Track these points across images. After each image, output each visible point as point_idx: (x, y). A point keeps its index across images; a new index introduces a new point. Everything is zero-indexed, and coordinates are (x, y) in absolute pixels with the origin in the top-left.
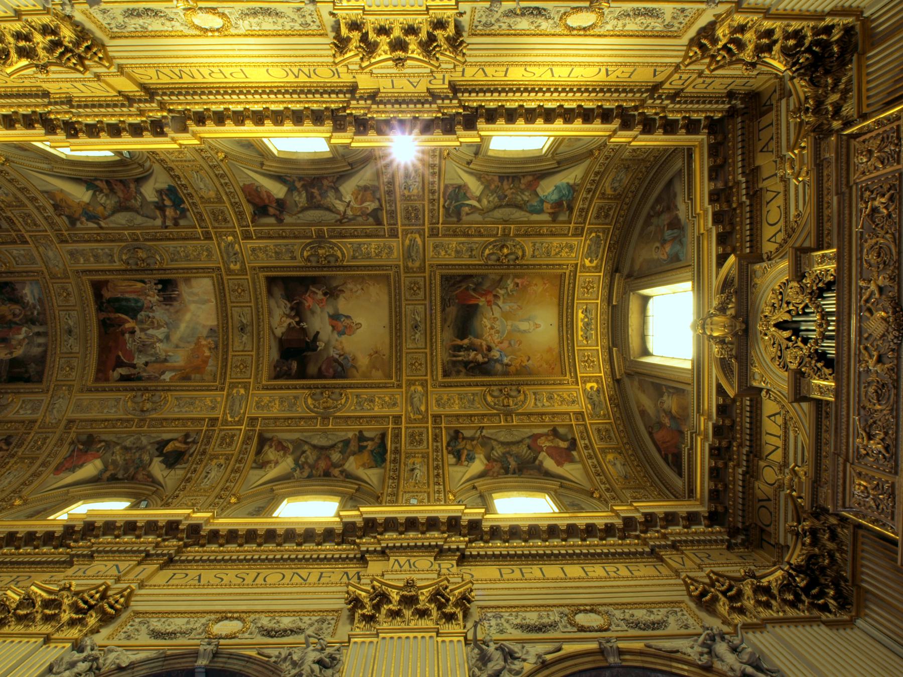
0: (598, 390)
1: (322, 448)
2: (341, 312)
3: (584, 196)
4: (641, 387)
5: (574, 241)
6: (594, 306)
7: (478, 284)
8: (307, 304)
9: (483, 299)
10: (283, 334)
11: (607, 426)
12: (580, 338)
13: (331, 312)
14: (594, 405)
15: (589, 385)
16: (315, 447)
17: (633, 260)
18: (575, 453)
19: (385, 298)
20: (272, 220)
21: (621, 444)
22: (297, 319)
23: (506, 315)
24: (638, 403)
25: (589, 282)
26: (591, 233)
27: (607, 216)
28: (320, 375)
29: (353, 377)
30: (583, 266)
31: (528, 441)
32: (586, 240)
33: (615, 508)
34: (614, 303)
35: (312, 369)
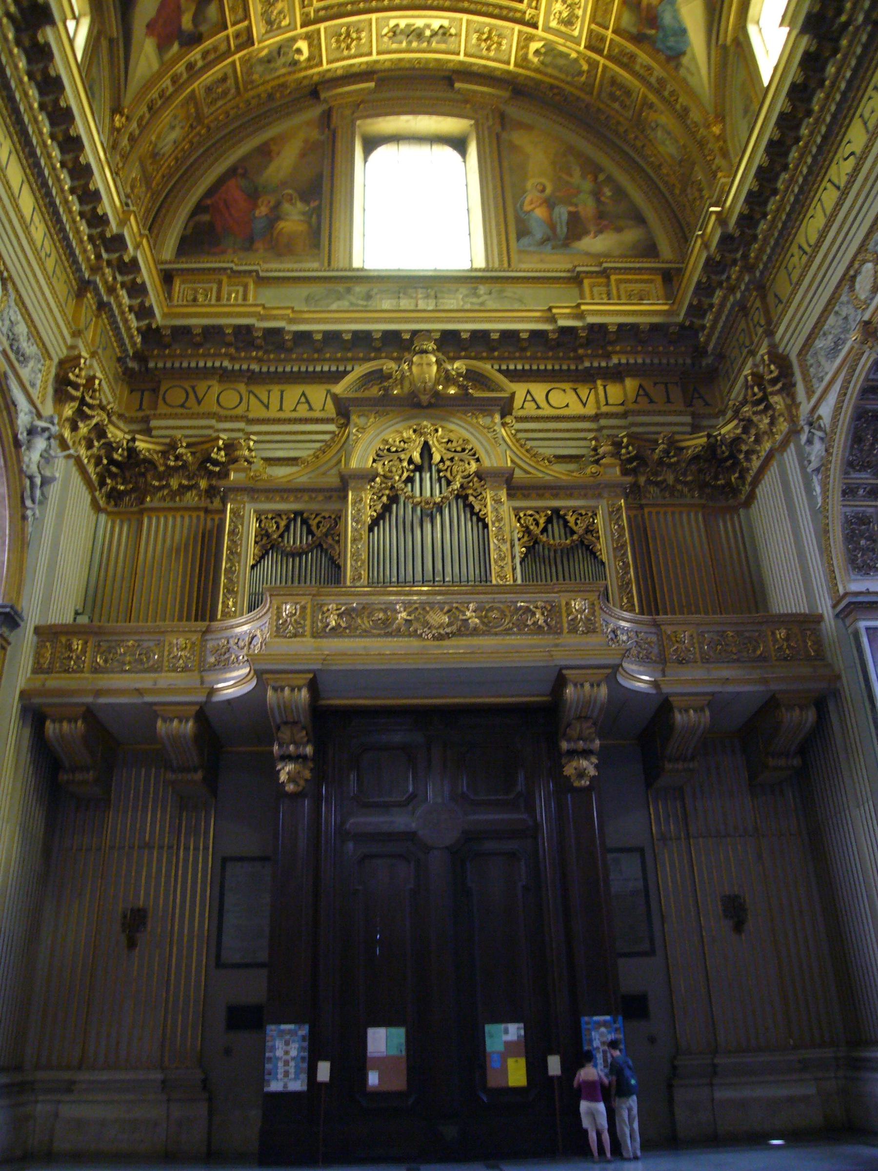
0: (295, 63)
3: (656, 74)
4: (309, 149)
5: (580, 30)
6: (452, 47)
11: (233, 91)
12: (392, 23)
14: (269, 60)
15: (303, 45)
17: (529, 128)
18: (176, 47)
21: (206, 121)
24: (280, 139)
25: (500, 44)
26: (589, 64)
27: (613, 97)
30: (530, 38)
32: (578, 52)
33: (132, 219)
34: (457, 85)
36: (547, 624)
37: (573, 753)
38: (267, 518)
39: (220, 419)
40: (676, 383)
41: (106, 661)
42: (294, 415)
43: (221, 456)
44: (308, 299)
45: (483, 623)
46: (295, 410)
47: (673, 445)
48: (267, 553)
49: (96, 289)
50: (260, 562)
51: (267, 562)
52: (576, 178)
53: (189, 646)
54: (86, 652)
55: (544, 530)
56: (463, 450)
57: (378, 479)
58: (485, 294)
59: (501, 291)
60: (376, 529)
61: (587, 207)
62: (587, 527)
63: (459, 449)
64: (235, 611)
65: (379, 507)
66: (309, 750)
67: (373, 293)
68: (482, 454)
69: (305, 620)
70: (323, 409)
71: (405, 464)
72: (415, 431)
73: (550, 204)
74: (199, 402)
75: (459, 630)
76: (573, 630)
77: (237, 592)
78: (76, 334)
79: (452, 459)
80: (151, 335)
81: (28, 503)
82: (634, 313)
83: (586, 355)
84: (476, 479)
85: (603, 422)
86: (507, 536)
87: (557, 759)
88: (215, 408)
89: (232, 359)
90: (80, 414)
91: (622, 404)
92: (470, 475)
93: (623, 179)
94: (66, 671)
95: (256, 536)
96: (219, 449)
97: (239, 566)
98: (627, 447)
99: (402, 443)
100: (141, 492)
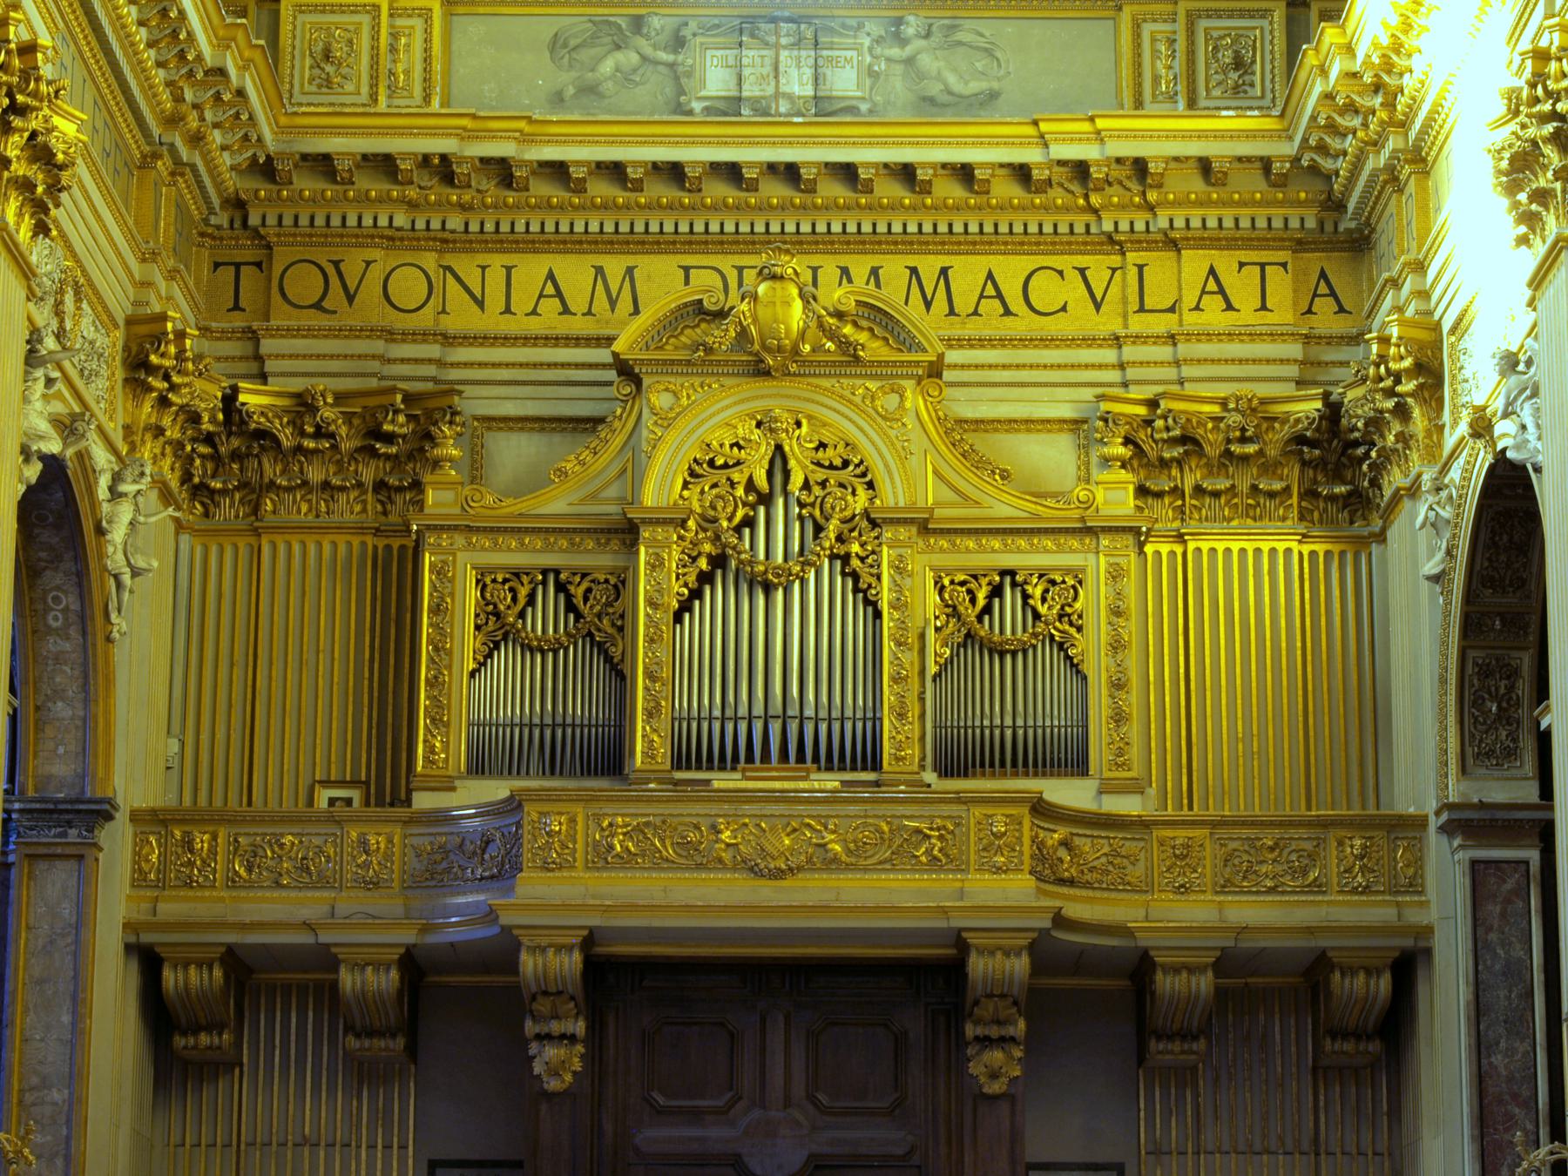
36: (947, 856)
37: (986, 1042)
38: (494, 581)
39: (390, 335)
40: (1284, 265)
41: (249, 870)
42: (534, 326)
43: (397, 425)
45: (849, 852)
46: (534, 312)
48: (497, 646)
49: (172, 147)
50: (484, 664)
51: (499, 659)
53: (382, 846)
54: (216, 854)
55: (988, 609)
56: (846, 463)
57: (691, 524)
58: (918, 36)
59: (953, 28)
60: (687, 616)
62: (1062, 608)
63: (838, 462)
64: (447, 759)
65: (692, 579)
66: (580, 1028)
67: (687, 32)
68: (879, 474)
69: (575, 842)
70: (589, 313)
71: (740, 492)
72: (759, 425)
74: (351, 298)
75: (809, 860)
77: (447, 725)
79: (823, 484)
81: (114, 617)
82: (1201, 135)
83: (1107, 206)
84: (865, 524)
86: (912, 639)
89: (412, 205)
90: (163, 402)
91: (1172, 310)
92: (854, 516)
94: (188, 885)
95: (477, 616)
96: (396, 412)
97: (450, 674)
98: (1165, 418)
99: (735, 449)
100: (253, 493)
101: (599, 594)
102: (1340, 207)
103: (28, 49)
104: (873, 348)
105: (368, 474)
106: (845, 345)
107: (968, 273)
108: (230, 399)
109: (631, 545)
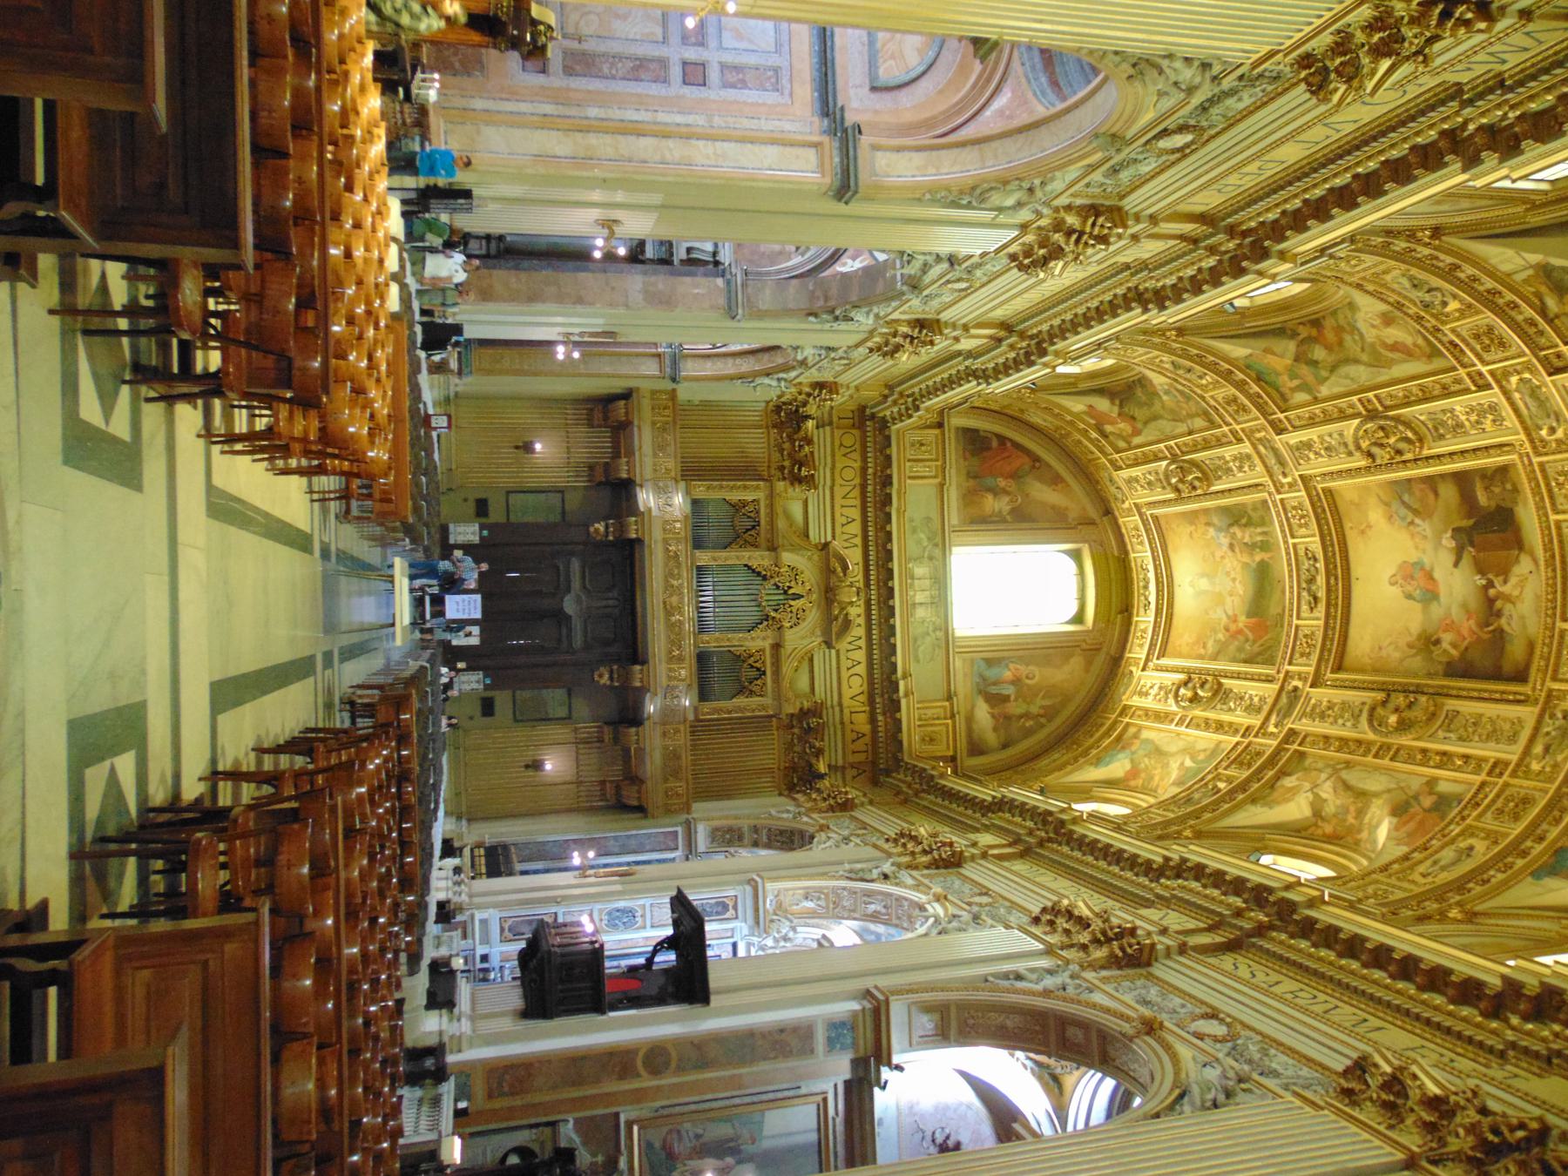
1: (1348, 361)
2: (1418, 606)
7: (1240, 650)
8: (1472, 623)
9: (1241, 625)
10: (1517, 561)
13: (1434, 608)
16: (1357, 361)
19: (1354, 632)
20: (1443, 787)
22: (1492, 592)
23: (1219, 599)
28: (1431, 482)
29: (1381, 485)
31: (1139, 425)
35: (1449, 492)
37: (611, 672)
42: (837, 515)
43: (804, 472)
44: (928, 519)
47: (819, 753)
51: (727, 507)
52: (1040, 702)
61: (1016, 708)
68: (795, 629)
73: (1016, 682)
76: (670, 670)
78: (857, 389)
80: (883, 424)
85: (837, 709)
87: (606, 660)
88: (839, 466)
90: (809, 395)
93: (1041, 735)
100: (779, 426)
101: (750, 539)
102: (888, 776)
103: (932, 343)
104: (835, 627)
105: (787, 463)
106: (836, 619)
107: (860, 655)
108: (808, 417)
109: (769, 549)
